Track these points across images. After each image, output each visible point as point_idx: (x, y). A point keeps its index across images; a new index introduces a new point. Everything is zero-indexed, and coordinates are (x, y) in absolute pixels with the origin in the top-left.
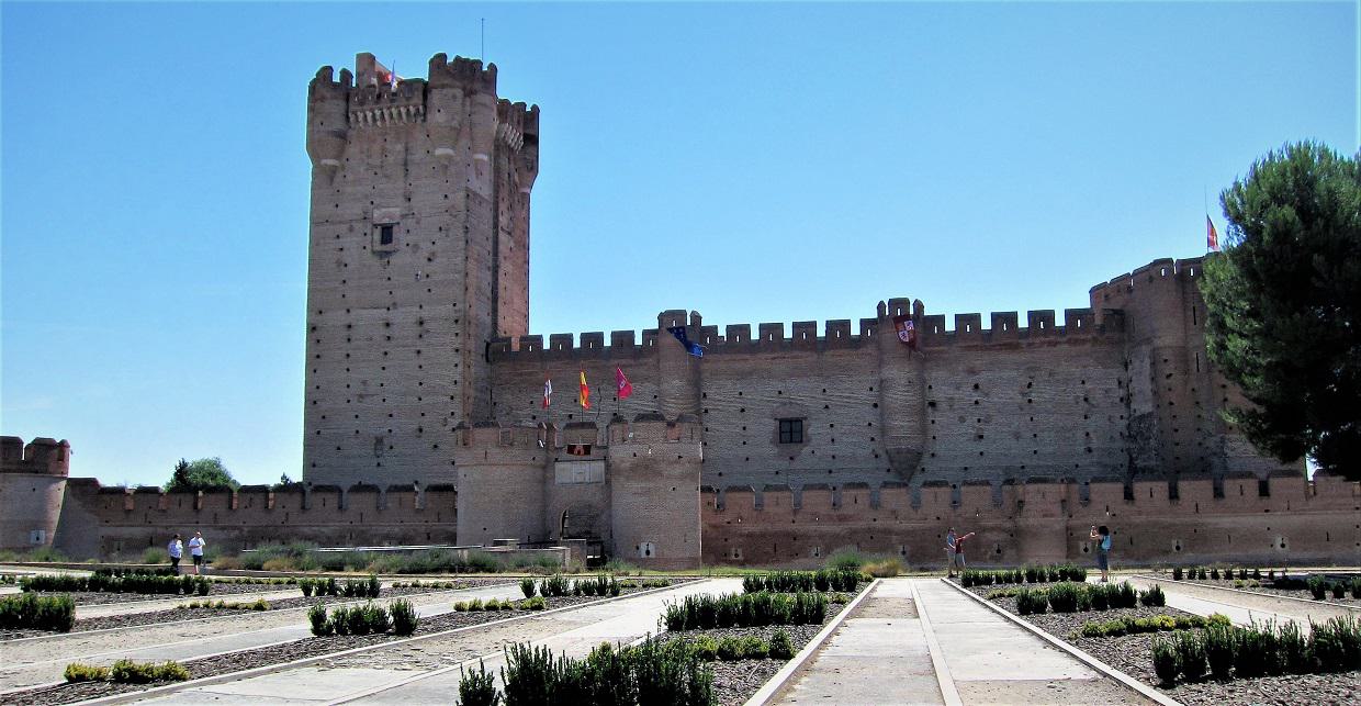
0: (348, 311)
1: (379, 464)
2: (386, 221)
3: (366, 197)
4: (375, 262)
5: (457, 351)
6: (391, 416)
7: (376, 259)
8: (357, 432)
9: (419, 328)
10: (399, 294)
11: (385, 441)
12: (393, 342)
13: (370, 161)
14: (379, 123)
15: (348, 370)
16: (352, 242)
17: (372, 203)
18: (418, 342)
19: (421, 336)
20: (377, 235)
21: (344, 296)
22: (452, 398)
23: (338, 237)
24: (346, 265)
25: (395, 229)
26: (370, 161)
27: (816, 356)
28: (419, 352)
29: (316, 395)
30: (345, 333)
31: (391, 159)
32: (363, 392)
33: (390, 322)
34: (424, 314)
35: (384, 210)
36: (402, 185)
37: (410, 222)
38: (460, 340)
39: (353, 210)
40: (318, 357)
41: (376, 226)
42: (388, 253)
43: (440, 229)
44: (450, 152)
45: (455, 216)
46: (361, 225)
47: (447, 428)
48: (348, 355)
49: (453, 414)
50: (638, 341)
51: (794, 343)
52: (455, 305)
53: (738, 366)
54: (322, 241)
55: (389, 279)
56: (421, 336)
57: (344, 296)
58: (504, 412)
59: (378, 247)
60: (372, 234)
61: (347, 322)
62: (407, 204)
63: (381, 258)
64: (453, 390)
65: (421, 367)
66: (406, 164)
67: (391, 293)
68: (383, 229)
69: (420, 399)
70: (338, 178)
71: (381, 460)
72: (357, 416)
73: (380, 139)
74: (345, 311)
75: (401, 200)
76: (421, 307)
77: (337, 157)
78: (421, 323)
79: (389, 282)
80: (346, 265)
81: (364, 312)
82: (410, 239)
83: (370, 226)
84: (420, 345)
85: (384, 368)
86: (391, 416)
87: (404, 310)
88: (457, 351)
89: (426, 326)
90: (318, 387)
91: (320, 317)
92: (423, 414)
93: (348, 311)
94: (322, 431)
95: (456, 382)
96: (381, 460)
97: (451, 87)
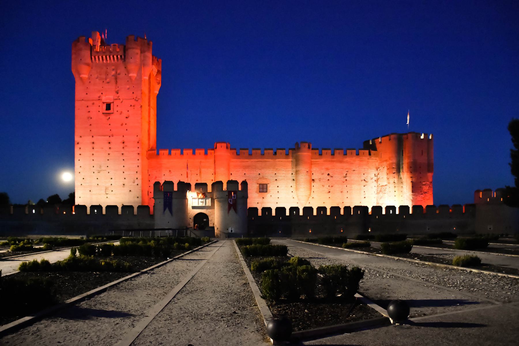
0: (93, 137)
1: (107, 197)
2: (108, 101)
5: (139, 154)
6: (112, 179)
7: (103, 117)
8: (98, 185)
11: (109, 189)
12: (111, 150)
14: (105, 61)
15: (93, 160)
18: (122, 150)
19: (123, 148)
20: (104, 106)
22: (137, 172)
24: (91, 118)
25: (112, 105)
28: (123, 154)
32: (100, 169)
38: (139, 149)
41: (104, 103)
43: (131, 106)
45: (137, 101)
48: (93, 154)
49: (137, 178)
56: (123, 148)
57: (91, 130)
60: (102, 106)
61: (92, 141)
63: (106, 116)
65: (124, 160)
67: (111, 130)
68: (107, 105)
69: (124, 172)
72: (97, 179)
74: (92, 137)
76: (123, 136)
78: (123, 143)
83: (101, 103)
86: (112, 179)
88: (139, 154)
89: (125, 144)
90: (81, 167)
91: (80, 139)
92: (125, 179)
93: (93, 137)
94: (83, 184)
95: (138, 166)
96: (108, 196)
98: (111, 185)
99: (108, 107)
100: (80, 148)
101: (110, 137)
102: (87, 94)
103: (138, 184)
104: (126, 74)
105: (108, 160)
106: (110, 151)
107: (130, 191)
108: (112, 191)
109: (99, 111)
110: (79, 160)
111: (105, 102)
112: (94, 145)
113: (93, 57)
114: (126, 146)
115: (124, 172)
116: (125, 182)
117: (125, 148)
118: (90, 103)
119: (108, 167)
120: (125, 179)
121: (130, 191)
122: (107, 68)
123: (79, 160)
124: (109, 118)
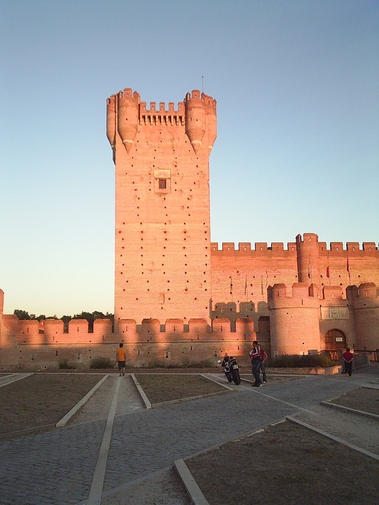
0: (141, 223)
1: (162, 308)
2: (162, 177)
3: (150, 163)
4: (158, 200)
5: (206, 248)
6: (169, 281)
8: (148, 290)
9: (184, 235)
10: (172, 217)
11: (165, 296)
12: (167, 242)
13: (152, 143)
15: (142, 256)
16: (142, 187)
17: (154, 166)
18: (184, 242)
19: (185, 239)
20: (157, 184)
21: (138, 215)
22: (204, 273)
23: (133, 183)
25: (168, 181)
26: (152, 143)
27: (376, 259)
29: (122, 269)
30: (140, 235)
31: (164, 143)
32: (152, 268)
33: (167, 231)
34: (187, 227)
35: (160, 170)
36: (173, 158)
37: (177, 179)
39: (143, 169)
40: (123, 248)
42: (166, 194)
43: (195, 183)
44: (200, 142)
46: (148, 178)
47: (202, 289)
48: (142, 248)
49: (205, 281)
50: (286, 248)
51: (346, 254)
52: (204, 224)
53: (337, 262)
54: (124, 185)
55: (165, 207)
56: (185, 239)
57: (138, 215)
58: (215, 282)
59: (158, 190)
62: (175, 168)
64: (205, 268)
66: (173, 148)
67: (167, 215)
69: (186, 273)
70: (132, 151)
71: (163, 306)
72: (148, 281)
73: (157, 133)
75: (171, 166)
77: (133, 140)
78: (185, 232)
79: (165, 209)
80: (139, 198)
81: (151, 225)
82: (176, 187)
83: (153, 178)
84: (185, 244)
85: (164, 256)
86: (169, 281)
87: (174, 225)
88: (206, 248)
89: (188, 234)
90: (123, 265)
92: (188, 281)
93: (141, 223)
94: (126, 290)
95: (206, 265)
96: (163, 306)
97: (202, 108)
98: (168, 290)
99: (163, 183)
100: (123, 239)
101: (165, 224)
102: (132, 166)
103: (206, 290)
104: (186, 142)
105: (164, 256)
106: (166, 244)
107: (196, 299)
108: (169, 299)
109: (150, 190)
110: (121, 256)
111: (158, 178)
112: (143, 235)
113: (141, 117)
114: (189, 237)
115: (186, 273)
116: (189, 285)
117: (187, 239)
118: (137, 179)
119: (163, 265)
120: (188, 281)
121: (196, 299)
122: (161, 133)
123: (121, 256)
124: (165, 199)
